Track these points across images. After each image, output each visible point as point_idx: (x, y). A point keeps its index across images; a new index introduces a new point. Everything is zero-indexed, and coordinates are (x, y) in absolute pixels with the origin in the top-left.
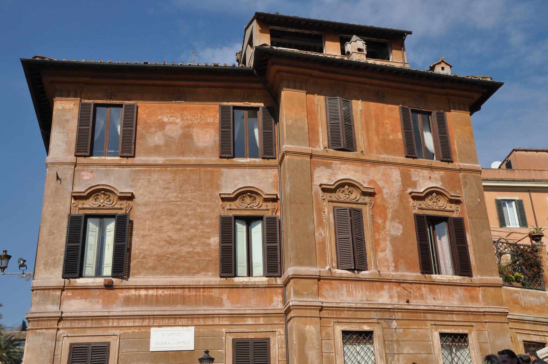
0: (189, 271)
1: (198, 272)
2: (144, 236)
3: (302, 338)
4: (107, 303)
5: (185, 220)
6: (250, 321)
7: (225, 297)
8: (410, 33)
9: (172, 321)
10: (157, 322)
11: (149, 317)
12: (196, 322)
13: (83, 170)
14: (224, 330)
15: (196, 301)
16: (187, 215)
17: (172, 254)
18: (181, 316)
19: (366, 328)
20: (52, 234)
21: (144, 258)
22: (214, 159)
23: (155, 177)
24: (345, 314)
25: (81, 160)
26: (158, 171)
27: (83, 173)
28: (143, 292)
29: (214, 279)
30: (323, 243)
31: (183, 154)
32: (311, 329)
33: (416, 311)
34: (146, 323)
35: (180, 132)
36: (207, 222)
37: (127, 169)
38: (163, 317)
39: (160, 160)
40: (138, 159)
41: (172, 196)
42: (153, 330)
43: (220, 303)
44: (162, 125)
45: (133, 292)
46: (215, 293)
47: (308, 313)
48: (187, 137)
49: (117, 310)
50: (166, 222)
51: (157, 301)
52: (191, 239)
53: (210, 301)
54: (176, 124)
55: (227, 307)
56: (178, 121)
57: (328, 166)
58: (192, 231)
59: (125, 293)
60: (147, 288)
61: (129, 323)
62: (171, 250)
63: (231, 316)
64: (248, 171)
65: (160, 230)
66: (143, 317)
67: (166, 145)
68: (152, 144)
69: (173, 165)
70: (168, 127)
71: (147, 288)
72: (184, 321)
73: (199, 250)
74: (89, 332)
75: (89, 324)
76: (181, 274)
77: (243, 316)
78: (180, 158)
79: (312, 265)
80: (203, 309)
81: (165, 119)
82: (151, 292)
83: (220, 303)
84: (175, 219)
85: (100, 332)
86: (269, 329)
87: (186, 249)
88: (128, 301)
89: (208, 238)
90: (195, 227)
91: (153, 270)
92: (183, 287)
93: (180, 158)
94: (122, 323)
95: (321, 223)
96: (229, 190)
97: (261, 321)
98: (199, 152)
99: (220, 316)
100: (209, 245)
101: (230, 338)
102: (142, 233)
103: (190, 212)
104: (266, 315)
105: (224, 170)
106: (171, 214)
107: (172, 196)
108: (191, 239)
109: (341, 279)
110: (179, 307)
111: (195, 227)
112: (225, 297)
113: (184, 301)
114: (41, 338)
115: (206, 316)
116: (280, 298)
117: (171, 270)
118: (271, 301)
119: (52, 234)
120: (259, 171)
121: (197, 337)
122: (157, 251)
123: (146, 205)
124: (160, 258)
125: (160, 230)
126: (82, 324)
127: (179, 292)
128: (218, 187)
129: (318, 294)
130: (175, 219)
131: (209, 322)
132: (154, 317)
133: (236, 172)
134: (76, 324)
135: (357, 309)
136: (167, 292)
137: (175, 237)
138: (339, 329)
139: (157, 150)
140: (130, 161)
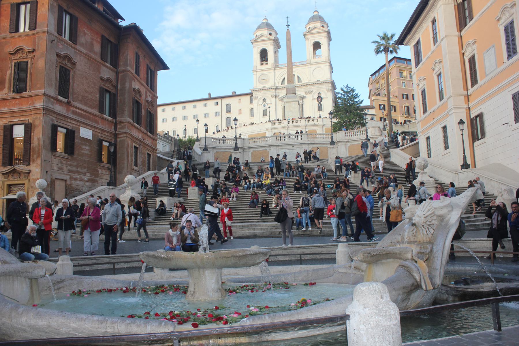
2: (78, 85)
4: (68, 110)
6: (106, 134)
8: (124, 20)
9: (86, 126)
10: (84, 126)
11: (81, 122)
12: (93, 129)
13: (59, 42)
14: (99, 135)
16: (91, 81)
17: (87, 97)
19: (138, 146)
20: (50, 70)
21: (78, 95)
22: (99, 59)
23: (82, 58)
26: (83, 56)
27: (59, 44)
28: (78, 110)
29: (96, 112)
33: (144, 143)
34: (79, 124)
36: (96, 87)
39: (84, 51)
40: (78, 47)
43: (98, 124)
45: (75, 109)
46: (97, 119)
48: (92, 44)
49: (71, 116)
50: (85, 82)
52: (92, 93)
54: (89, 36)
55: (100, 126)
56: (90, 34)
58: (92, 89)
62: (86, 95)
63: (102, 130)
64: (108, 70)
66: (78, 121)
69: (88, 56)
70: (86, 36)
71: (79, 109)
72: (89, 127)
73: (93, 98)
74: (62, 122)
76: (89, 107)
77: (104, 131)
78: (90, 53)
80: (95, 125)
81: (86, 32)
82: (80, 111)
83: (98, 124)
84: (88, 81)
85: (65, 123)
87: (90, 97)
88: (74, 113)
89: (96, 94)
91: (81, 102)
93: (90, 53)
94: (72, 121)
98: (95, 53)
100: (96, 97)
103: (92, 80)
104: (110, 133)
106: (87, 79)
108: (92, 93)
110: (88, 121)
113: (89, 119)
114: (48, 118)
115: (96, 128)
117: (86, 104)
118: (111, 128)
119: (50, 70)
120: (111, 72)
121: (93, 135)
123: (79, 70)
126: (60, 117)
128: (100, 73)
130: (88, 81)
136: (84, 113)
138: (134, 144)
139: (82, 45)
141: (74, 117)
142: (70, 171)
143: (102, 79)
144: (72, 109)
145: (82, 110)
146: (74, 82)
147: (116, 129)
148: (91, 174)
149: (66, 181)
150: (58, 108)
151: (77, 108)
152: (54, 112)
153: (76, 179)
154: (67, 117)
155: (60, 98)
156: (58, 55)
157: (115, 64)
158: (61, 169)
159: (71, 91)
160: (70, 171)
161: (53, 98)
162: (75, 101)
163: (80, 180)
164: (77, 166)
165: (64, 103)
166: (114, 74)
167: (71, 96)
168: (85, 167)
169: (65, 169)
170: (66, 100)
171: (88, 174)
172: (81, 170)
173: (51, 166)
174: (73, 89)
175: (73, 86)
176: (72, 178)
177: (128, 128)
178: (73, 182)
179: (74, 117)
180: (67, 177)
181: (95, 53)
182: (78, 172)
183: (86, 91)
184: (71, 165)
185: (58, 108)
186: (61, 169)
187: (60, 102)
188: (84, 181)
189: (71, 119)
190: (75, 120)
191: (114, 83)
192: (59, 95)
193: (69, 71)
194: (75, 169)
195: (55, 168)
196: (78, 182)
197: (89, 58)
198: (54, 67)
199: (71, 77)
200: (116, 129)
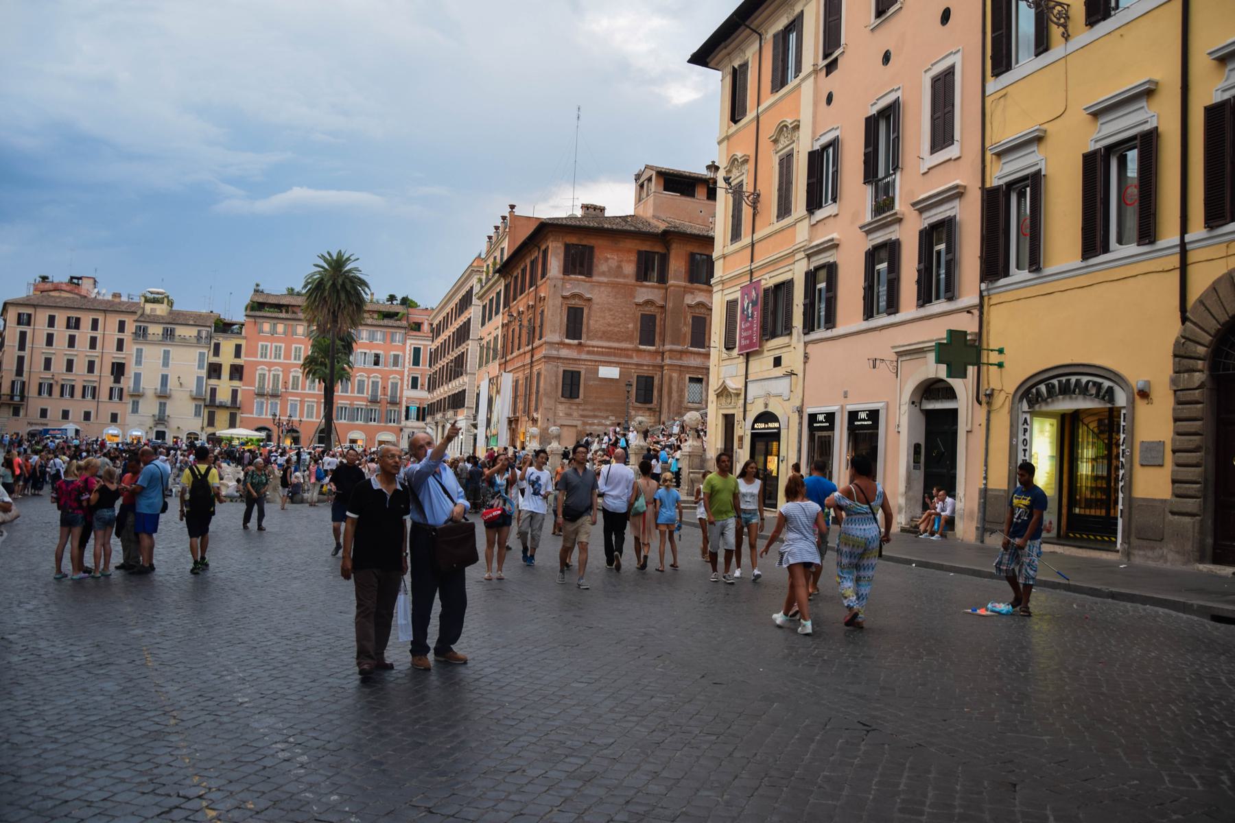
0: (618, 340)
1: (622, 341)
2: (597, 321)
3: (671, 379)
4: (579, 353)
5: (617, 314)
6: (645, 368)
7: (634, 355)
15: (620, 356)
18: (613, 362)
19: (700, 376)
22: (633, 281)
23: (602, 289)
24: (691, 370)
25: (566, 277)
28: (596, 349)
30: (685, 334)
31: (617, 277)
32: (675, 375)
35: (616, 264)
37: (589, 284)
38: (605, 362)
39: (604, 279)
40: (595, 278)
41: (611, 300)
42: (600, 368)
44: (607, 259)
45: (591, 349)
46: (630, 353)
47: (675, 368)
48: (619, 267)
49: (584, 356)
51: (602, 354)
53: (628, 356)
55: (635, 360)
56: (616, 257)
57: (692, 293)
59: (587, 349)
60: (598, 347)
61: (589, 363)
62: (609, 329)
63: (637, 365)
64: (649, 290)
65: (604, 318)
66: (596, 361)
67: (609, 271)
68: (601, 270)
70: (610, 261)
71: (598, 347)
73: (623, 330)
74: (571, 366)
75: (571, 362)
77: (642, 365)
78: (616, 280)
79: (678, 345)
80: (623, 360)
81: (609, 256)
83: (631, 357)
84: (612, 313)
86: (654, 372)
87: (616, 329)
88: (589, 353)
90: (621, 318)
91: (601, 338)
92: (615, 348)
95: (685, 324)
96: (640, 300)
97: (651, 368)
98: (625, 277)
99: (631, 364)
101: (636, 375)
102: (595, 319)
104: (654, 366)
105: (638, 288)
106: (610, 310)
107: (611, 300)
109: (692, 353)
111: (621, 318)
112: (634, 355)
113: (615, 355)
115: (625, 364)
116: (660, 358)
117: (609, 339)
120: (656, 290)
122: (603, 329)
123: (598, 304)
124: (604, 333)
125: (604, 318)
127: (613, 350)
128: (634, 298)
129: (680, 359)
131: (626, 366)
132: (601, 361)
133: (644, 290)
134: (565, 361)
135: (697, 368)
137: (612, 322)
138: (687, 376)
139: (603, 274)
140: (590, 279)
141: (588, 357)
142: (582, 416)
143: (638, 305)
144: (586, 349)
145: (602, 347)
146: (589, 319)
147: (663, 360)
148: (617, 417)
149: (576, 426)
150: (564, 353)
151: (593, 347)
152: (559, 358)
153: (593, 424)
154: (579, 360)
155: (567, 341)
156: (564, 297)
157: (662, 279)
158: (569, 415)
159: (584, 329)
160: (582, 416)
161: (558, 344)
162: (591, 340)
163: (598, 425)
164: (594, 410)
165: (574, 345)
166: (664, 291)
167: (584, 336)
168: (607, 411)
169: (575, 414)
170: (576, 342)
171: (613, 418)
172: (599, 414)
173: (555, 413)
174: (588, 328)
175: (588, 323)
176: (585, 424)
177: (670, 358)
178: (588, 427)
179: (588, 357)
180: (579, 423)
181: (625, 277)
182: (595, 417)
183: (609, 325)
184: (583, 410)
185: (564, 353)
186: (569, 415)
187: (569, 345)
188: (606, 425)
189: (585, 360)
190: (591, 361)
191: (661, 303)
192: (567, 338)
193: (582, 309)
194: (592, 413)
195: (561, 415)
196: (595, 427)
197: (614, 285)
198: (559, 310)
199: (585, 315)
200: (663, 360)
